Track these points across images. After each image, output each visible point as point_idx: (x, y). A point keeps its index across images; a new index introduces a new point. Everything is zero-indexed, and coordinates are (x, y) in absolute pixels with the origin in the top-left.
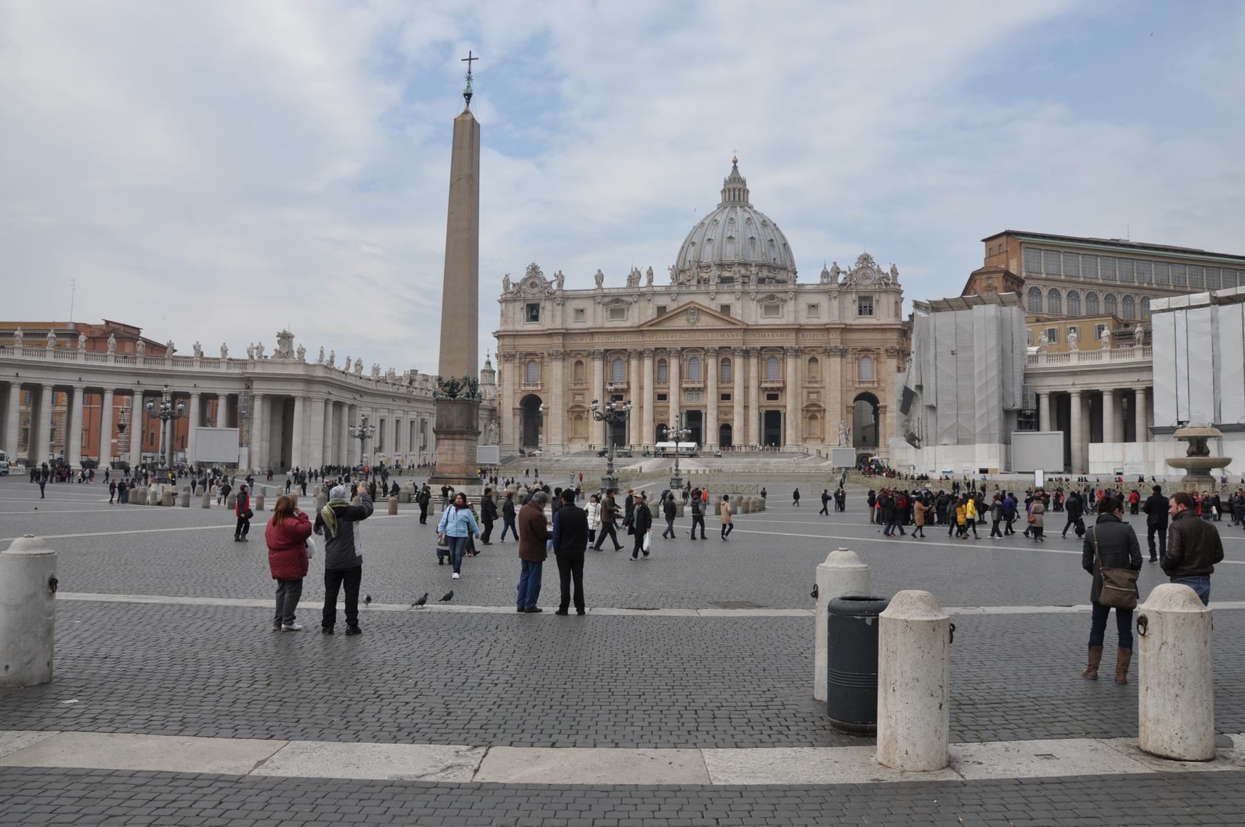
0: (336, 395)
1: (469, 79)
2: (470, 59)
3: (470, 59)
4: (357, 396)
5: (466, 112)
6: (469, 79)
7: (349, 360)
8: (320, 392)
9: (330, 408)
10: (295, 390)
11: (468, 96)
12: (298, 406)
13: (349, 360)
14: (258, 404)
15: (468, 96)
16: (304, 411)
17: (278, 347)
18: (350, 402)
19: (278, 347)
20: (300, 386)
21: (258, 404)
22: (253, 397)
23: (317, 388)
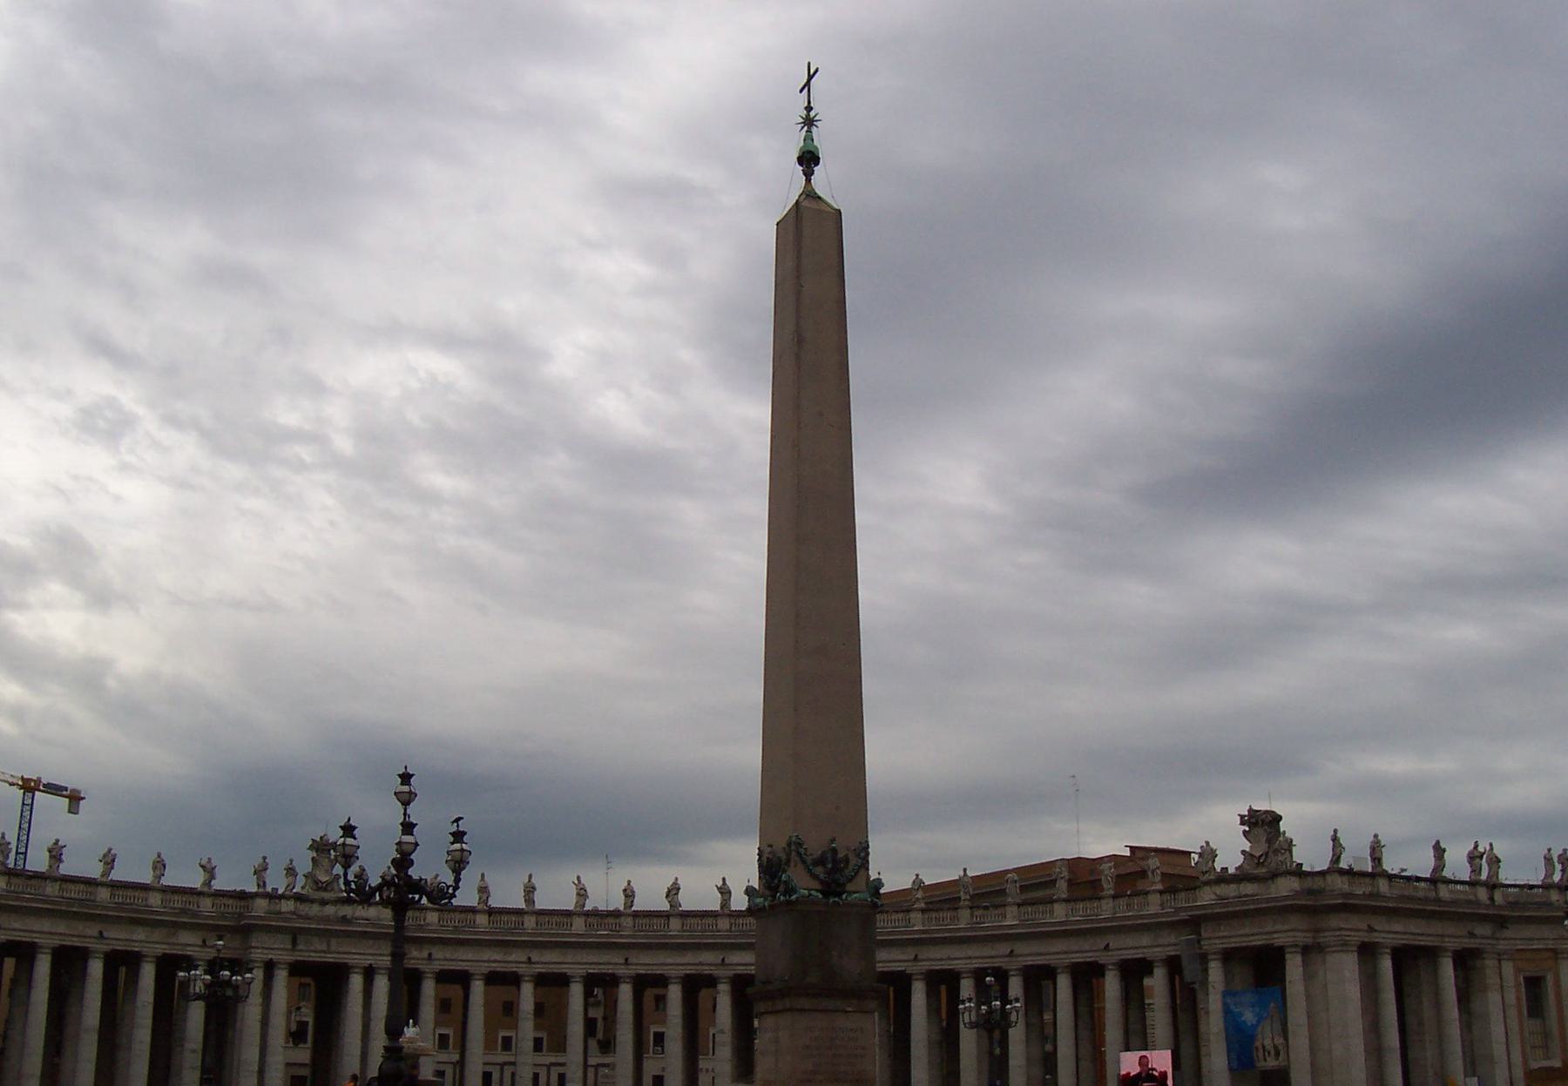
0: (1393, 932)
1: (809, 122)
2: (810, 77)
3: (810, 77)
4: (1483, 930)
5: (809, 194)
6: (809, 122)
7: (1439, 851)
8: (1355, 927)
9: (1386, 964)
10: (1283, 933)
11: (809, 159)
12: (1294, 967)
13: (1439, 851)
14: (1215, 972)
15: (809, 159)
16: (1308, 976)
17: (1247, 846)
18: (1452, 944)
19: (1247, 846)
20: (1295, 921)
21: (1215, 972)
22: (1204, 959)
23: (1335, 921)
